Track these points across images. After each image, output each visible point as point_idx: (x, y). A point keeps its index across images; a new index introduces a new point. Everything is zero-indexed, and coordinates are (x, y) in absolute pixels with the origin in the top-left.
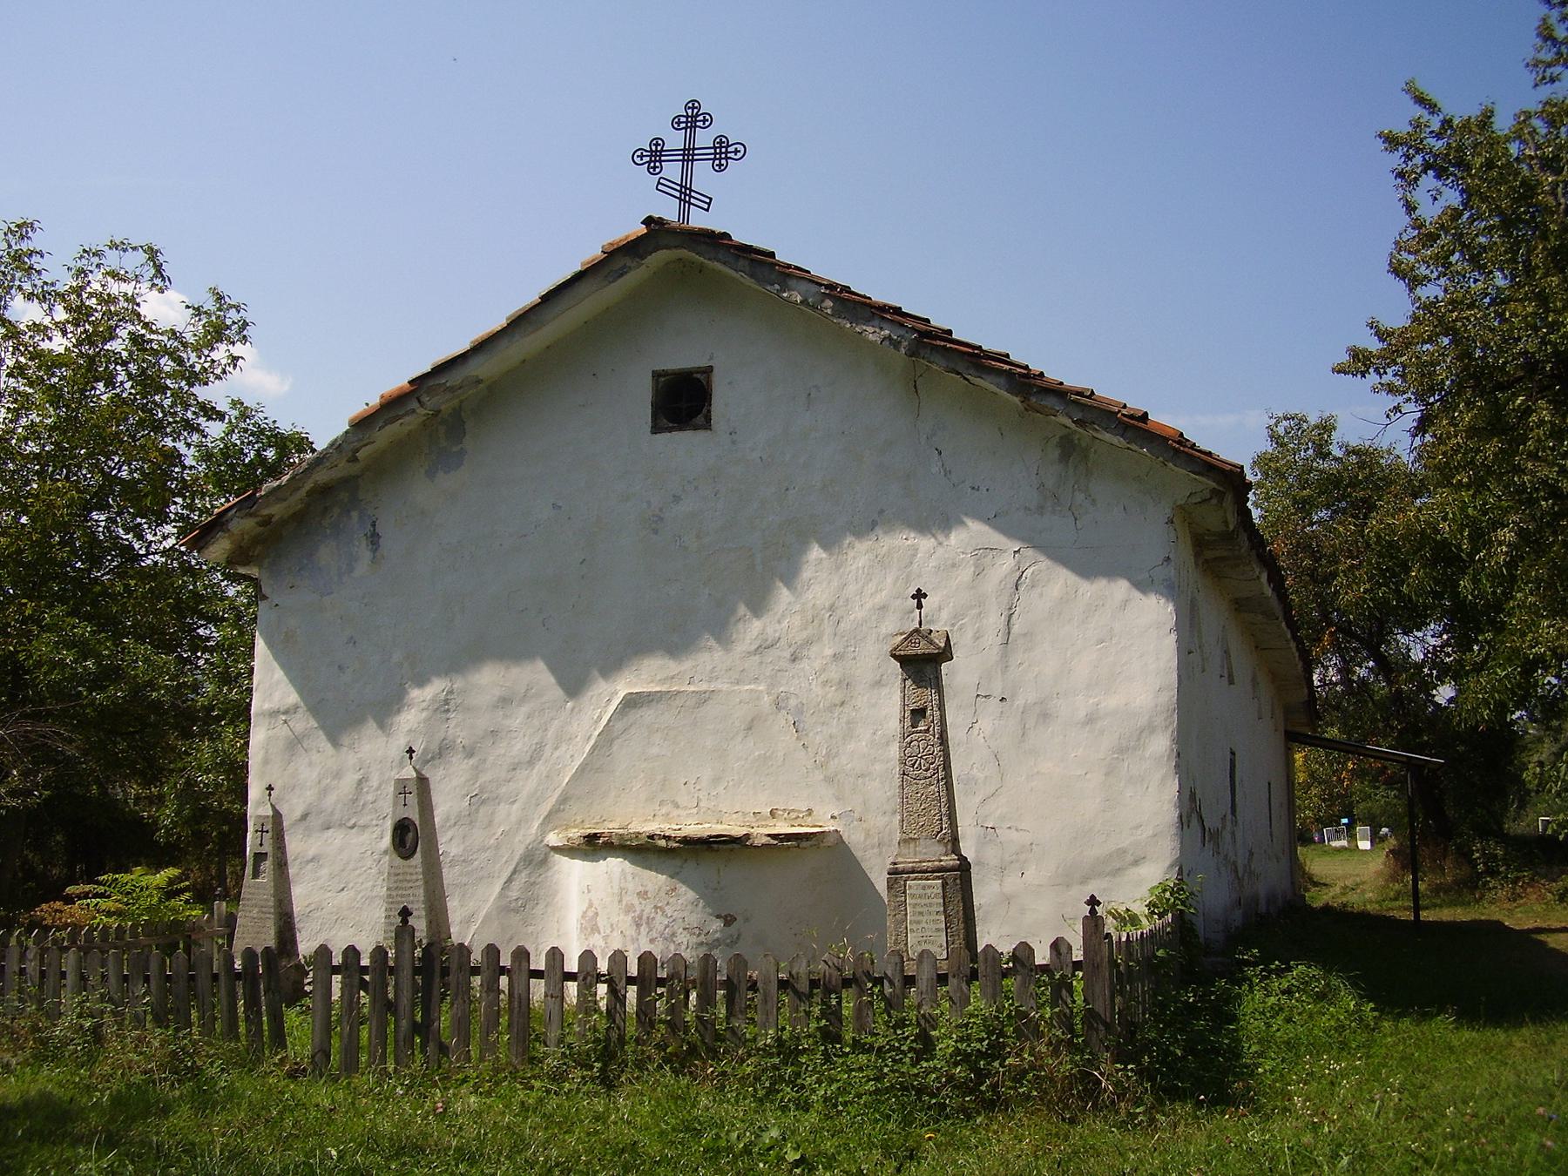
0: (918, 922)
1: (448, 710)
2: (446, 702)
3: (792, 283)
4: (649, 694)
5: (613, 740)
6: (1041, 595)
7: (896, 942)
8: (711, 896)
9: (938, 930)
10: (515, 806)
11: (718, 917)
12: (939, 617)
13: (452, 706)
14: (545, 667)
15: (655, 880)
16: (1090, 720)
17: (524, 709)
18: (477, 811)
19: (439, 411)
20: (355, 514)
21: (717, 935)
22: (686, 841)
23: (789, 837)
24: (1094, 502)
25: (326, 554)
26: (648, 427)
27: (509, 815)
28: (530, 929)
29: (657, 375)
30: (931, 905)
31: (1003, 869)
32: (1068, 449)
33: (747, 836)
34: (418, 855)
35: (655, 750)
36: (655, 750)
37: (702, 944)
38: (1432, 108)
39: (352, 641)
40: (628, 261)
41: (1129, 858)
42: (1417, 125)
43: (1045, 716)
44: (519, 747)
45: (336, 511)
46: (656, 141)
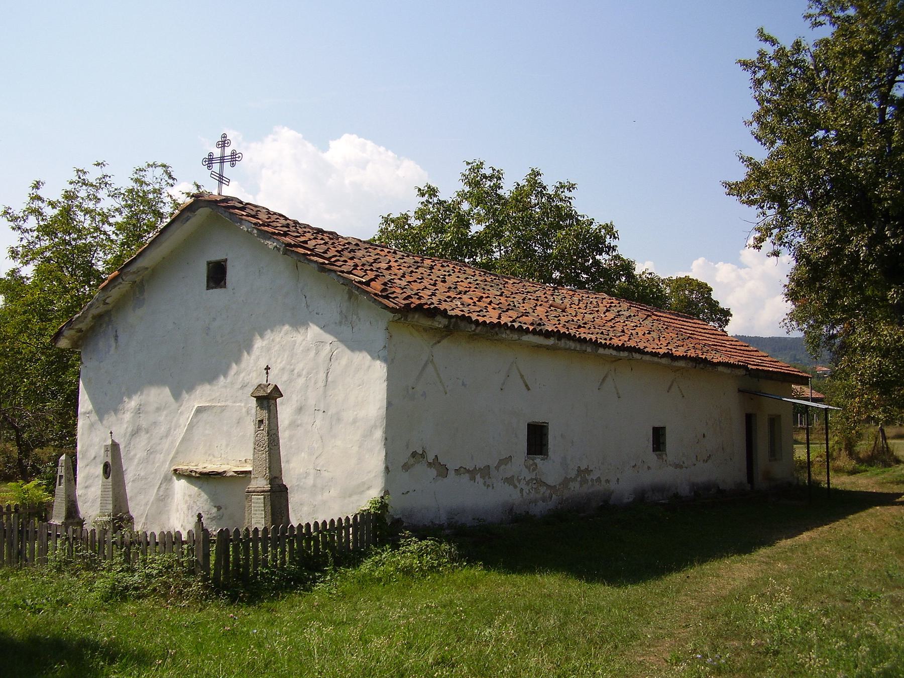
0: (255, 514)
1: (140, 413)
2: (139, 409)
3: (244, 222)
4: (205, 407)
5: (193, 427)
6: (339, 364)
7: (248, 523)
8: (214, 498)
9: (262, 518)
10: (162, 455)
11: (215, 507)
12: (276, 379)
13: (141, 411)
14: (170, 394)
15: (194, 489)
16: (355, 421)
17: (165, 413)
18: (149, 457)
19: (135, 282)
20: (110, 326)
21: (214, 515)
22: (201, 473)
23: (242, 472)
24: (359, 320)
25: (101, 344)
26: (205, 288)
27: (160, 458)
28: (167, 508)
29: (209, 263)
30: (260, 507)
31: (323, 489)
32: (351, 295)
33: (225, 472)
34: (110, 477)
35: (207, 432)
36: (207, 432)
37: (209, 518)
38: (773, 42)
39: (110, 383)
40: (189, 214)
41: (366, 486)
42: (762, 54)
43: (339, 420)
44: (163, 429)
45: (104, 326)
46: (211, 154)
